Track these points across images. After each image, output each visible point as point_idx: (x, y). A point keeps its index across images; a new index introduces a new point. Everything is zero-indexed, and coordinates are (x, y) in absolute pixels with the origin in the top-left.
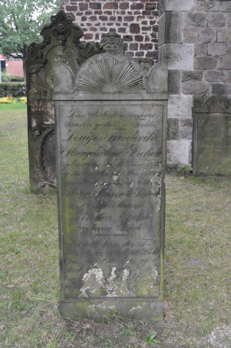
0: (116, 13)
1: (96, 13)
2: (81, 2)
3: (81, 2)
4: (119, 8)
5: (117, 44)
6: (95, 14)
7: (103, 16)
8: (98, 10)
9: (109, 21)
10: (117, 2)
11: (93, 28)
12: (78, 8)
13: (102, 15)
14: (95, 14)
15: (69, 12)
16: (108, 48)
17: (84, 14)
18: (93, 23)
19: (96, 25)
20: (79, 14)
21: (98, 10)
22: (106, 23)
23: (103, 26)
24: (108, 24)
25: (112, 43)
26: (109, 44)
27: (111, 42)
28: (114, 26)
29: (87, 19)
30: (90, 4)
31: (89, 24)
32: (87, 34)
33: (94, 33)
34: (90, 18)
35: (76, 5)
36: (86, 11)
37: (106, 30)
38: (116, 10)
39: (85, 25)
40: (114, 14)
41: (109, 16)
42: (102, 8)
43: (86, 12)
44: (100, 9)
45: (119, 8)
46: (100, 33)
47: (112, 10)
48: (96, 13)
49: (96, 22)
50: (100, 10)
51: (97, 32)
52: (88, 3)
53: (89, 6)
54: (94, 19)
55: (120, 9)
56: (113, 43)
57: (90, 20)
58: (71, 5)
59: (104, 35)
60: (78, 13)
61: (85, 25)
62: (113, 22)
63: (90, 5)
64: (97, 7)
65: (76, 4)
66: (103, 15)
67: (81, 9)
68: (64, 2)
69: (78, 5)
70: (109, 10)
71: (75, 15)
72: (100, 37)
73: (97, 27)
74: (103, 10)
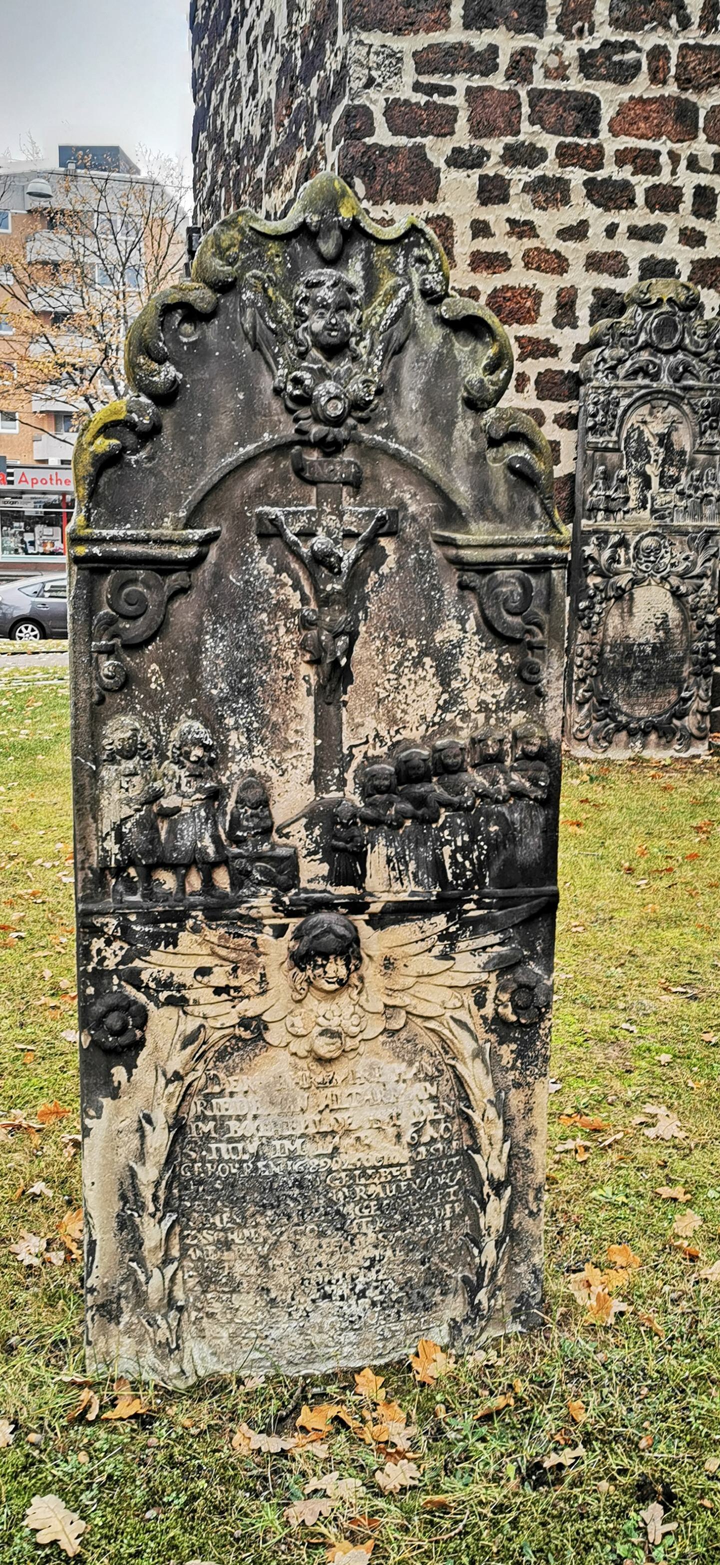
0: (683, 163)
1: (566, 155)
2: (477, 81)
3: (477, 81)
4: (702, 137)
5: (697, 355)
6: (562, 166)
7: (607, 181)
8: (583, 142)
9: (641, 216)
10: (690, 96)
11: (547, 251)
12: (462, 124)
13: (601, 175)
14: (562, 166)
15: (402, 141)
16: (641, 381)
17: (494, 159)
18: (549, 222)
19: (567, 234)
20: (461, 159)
21: (583, 142)
22: (623, 228)
23: (603, 246)
24: (635, 233)
25: (665, 346)
26: (645, 355)
27: (660, 340)
28: (670, 248)
29: (512, 191)
30: (536, 96)
31: (521, 229)
32: (505, 288)
33: (548, 285)
34: (528, 188)
35: (449, 101)
36: (509, 139)
37: (621, 272)
38: (684, 150)
39: (500, 228)
40: (674, 173)
41: (641, 184)
42: (604, 126)
43: (507, 147)
44: (595, 133)
45: (702, 137)
46: (587, 284)
47: (663, 146)
48: (566, 155)
49: (568, 216)
50: (594, 141)
51: (565, 281)
52: (523, 94)
53: (526, 110)
54: (551, 192)
55: (709, 141)
56: (672, 352)
57: (527, 198)
58: (422, 99)
59: (607, 304)
60: (457, 151)
61: (500, 228)
62: (668, 220)
63: (532, 106)
64: (572, 118)
65: (451, 91)
66: (610, 171)
67: (478, 130)
68: (374, 73)
69: (458, 100)
70: (643, 144)
71: (443, 166)
72: (583, 312)
73: (568, 248)
74: (611, 145)
